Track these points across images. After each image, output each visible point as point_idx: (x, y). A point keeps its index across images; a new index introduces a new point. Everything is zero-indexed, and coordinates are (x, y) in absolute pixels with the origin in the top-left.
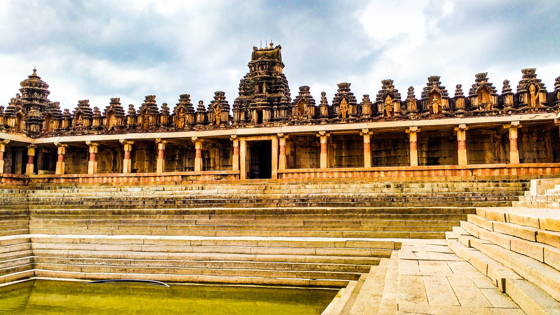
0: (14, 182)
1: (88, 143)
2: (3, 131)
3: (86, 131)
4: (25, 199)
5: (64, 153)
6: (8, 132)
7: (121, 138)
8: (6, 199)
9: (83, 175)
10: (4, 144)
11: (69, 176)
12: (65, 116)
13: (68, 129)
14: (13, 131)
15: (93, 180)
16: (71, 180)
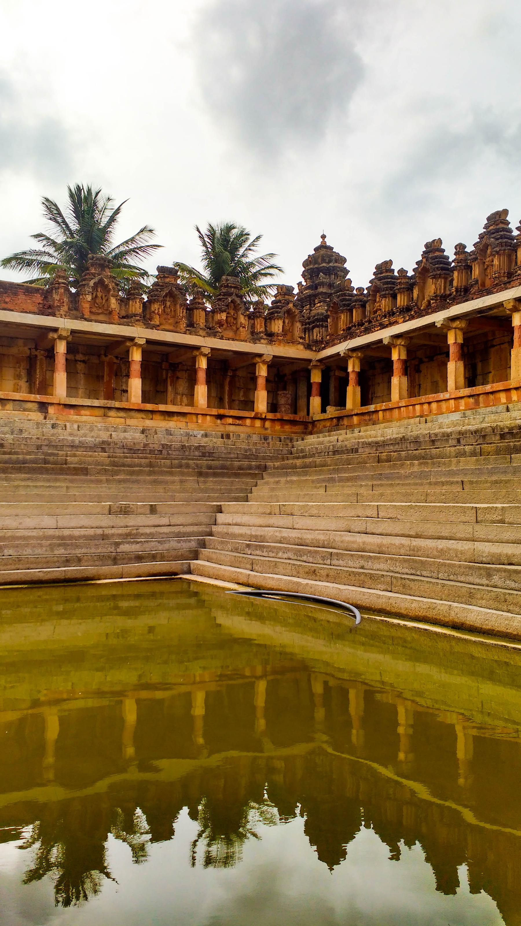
0: (287, 428)
1: (386, 342)
2: (262, 341)
3: (386, 321)
4: (285, 452)
5: (357, 369)
6: (271, 342)
7: (438, 318)
8: (250, 450)
9: (384, 406)
10: (264, 362)
11: (365, 409)
12: (356, 301)
13: (361, 324)
14: (280, 341)
15: (400, 413)
16: (367, 417)
